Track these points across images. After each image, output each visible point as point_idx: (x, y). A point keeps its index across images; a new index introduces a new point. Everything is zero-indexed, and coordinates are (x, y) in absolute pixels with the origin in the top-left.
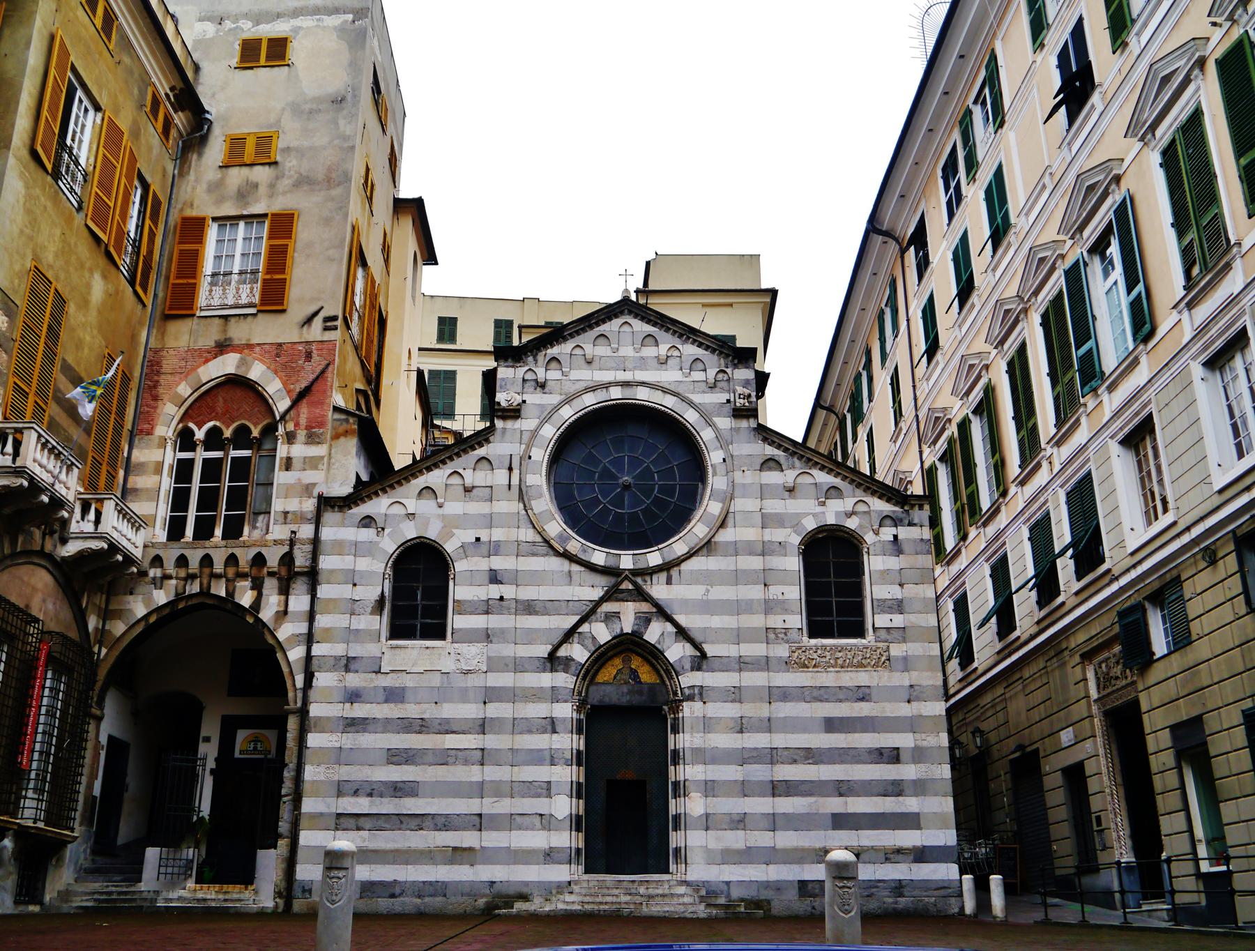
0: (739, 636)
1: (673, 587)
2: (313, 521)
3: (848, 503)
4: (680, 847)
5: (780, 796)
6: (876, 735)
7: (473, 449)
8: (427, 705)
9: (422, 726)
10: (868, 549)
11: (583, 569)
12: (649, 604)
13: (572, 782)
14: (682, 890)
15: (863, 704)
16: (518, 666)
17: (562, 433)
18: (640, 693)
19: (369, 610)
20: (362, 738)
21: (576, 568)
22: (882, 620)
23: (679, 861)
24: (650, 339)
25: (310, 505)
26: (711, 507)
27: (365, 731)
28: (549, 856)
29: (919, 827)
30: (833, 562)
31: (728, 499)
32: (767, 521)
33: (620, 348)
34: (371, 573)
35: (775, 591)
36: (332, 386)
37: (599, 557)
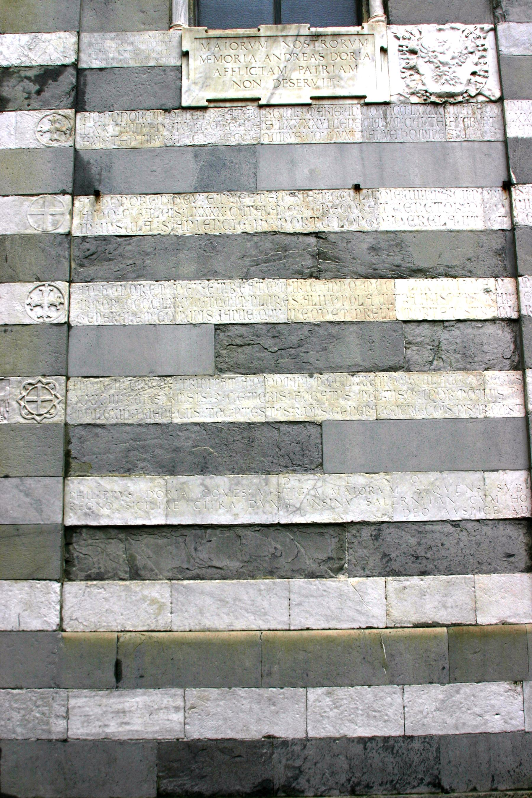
8: (328, 197)
9: (320, 255)
20: (135, 294)
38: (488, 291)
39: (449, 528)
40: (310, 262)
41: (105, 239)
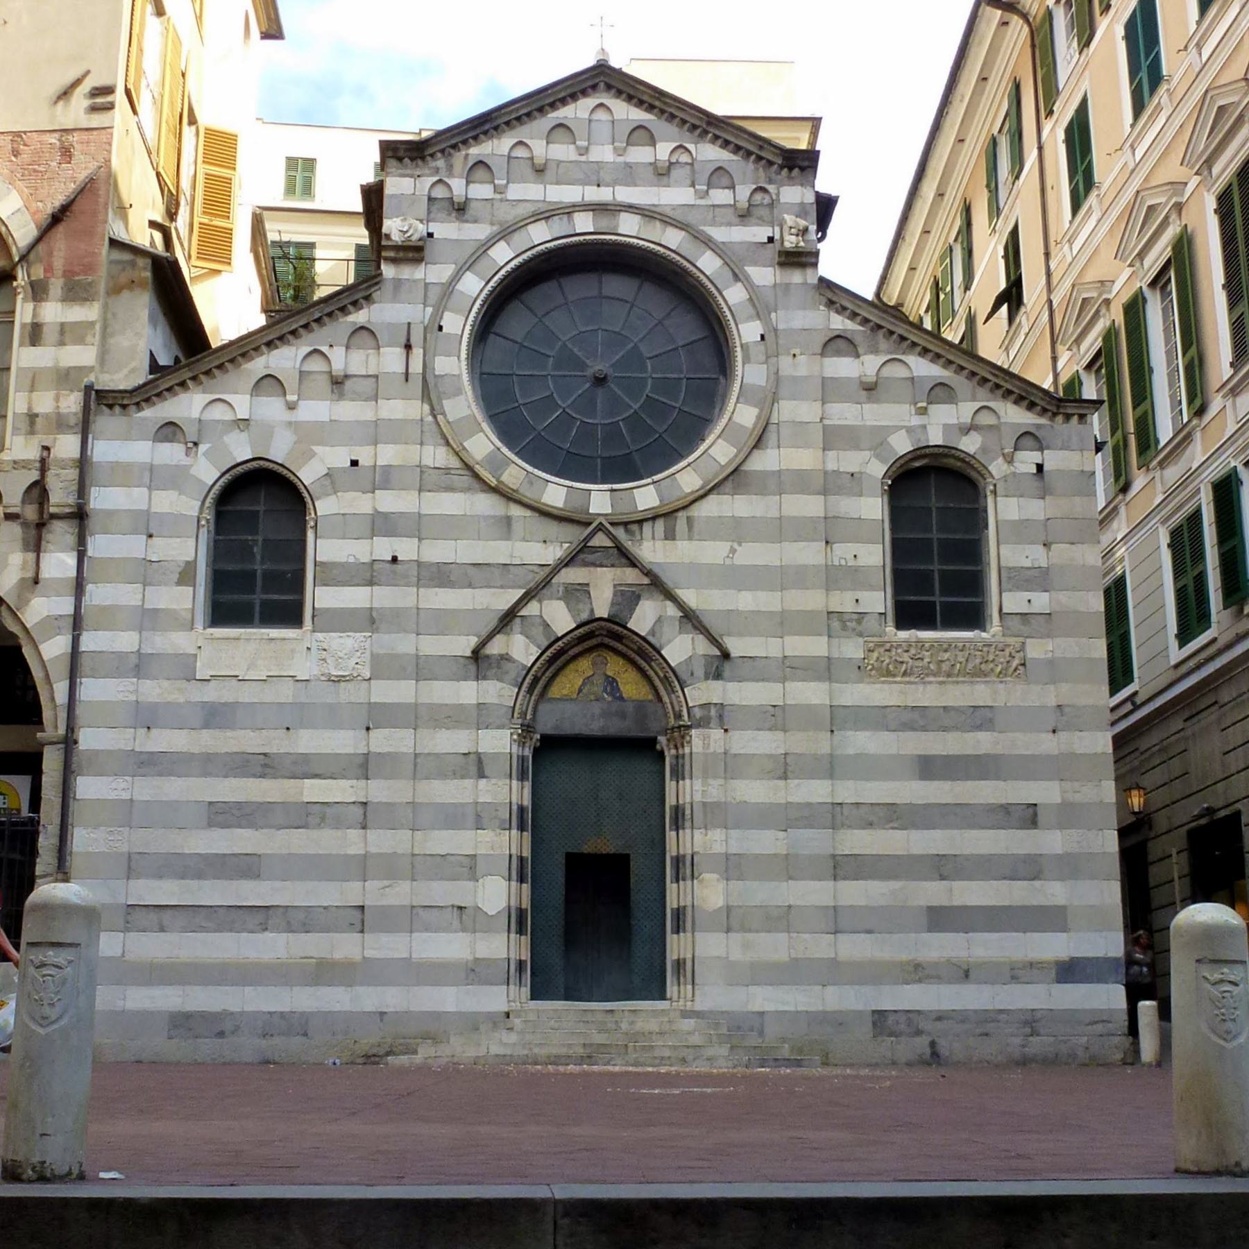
0: (784, 623)
1: (679, 543)
2: (79, 428)
3: (964, 411)
4: (685, 960)
5: (845, 879)
6: (1001, 784)
7: (343, 310)
8: (272, 733)
9: (265, 766)
10: (995, 485)
11: (528, 513)
12: (636, 571)
13: (510, 856)
14: (688, 1024)
15: (983, 736)
16: (422, 669)
17: (495, 288)
18: (622, 715)
19: (175, 577)
21: (516, 511)
22: (1015, 602)
23: (682, 979)
24: (641, 135)
25: (72, 403)
26: (743, 415)
27: (171, 773)
28: (475, 972)
29: (1064, 929)
30: (937, 508)
31: (769, 400)
32: (833, 437)
33: (592, 148)
34: (178, 518)
35: (843, 552)
36: (106, 204)
37: (556, 493)
38: (352, 787)
39: (322, 910)
40: (260, 769)
41: (152, 753)
